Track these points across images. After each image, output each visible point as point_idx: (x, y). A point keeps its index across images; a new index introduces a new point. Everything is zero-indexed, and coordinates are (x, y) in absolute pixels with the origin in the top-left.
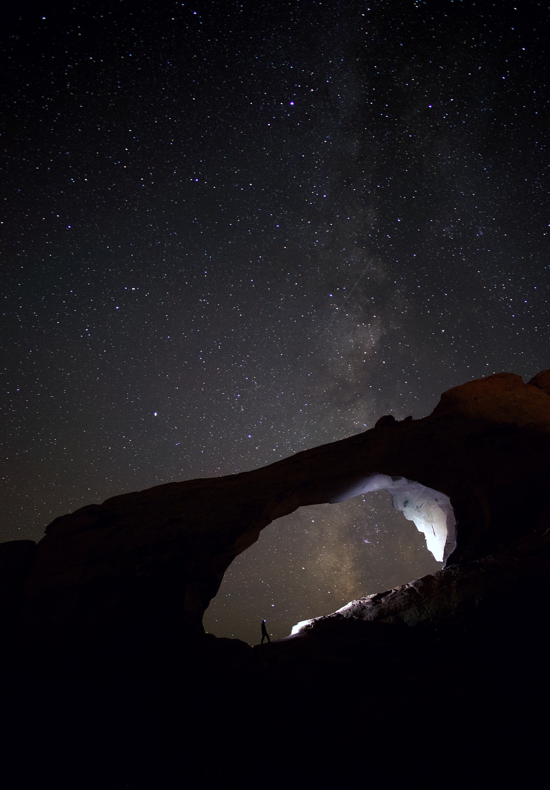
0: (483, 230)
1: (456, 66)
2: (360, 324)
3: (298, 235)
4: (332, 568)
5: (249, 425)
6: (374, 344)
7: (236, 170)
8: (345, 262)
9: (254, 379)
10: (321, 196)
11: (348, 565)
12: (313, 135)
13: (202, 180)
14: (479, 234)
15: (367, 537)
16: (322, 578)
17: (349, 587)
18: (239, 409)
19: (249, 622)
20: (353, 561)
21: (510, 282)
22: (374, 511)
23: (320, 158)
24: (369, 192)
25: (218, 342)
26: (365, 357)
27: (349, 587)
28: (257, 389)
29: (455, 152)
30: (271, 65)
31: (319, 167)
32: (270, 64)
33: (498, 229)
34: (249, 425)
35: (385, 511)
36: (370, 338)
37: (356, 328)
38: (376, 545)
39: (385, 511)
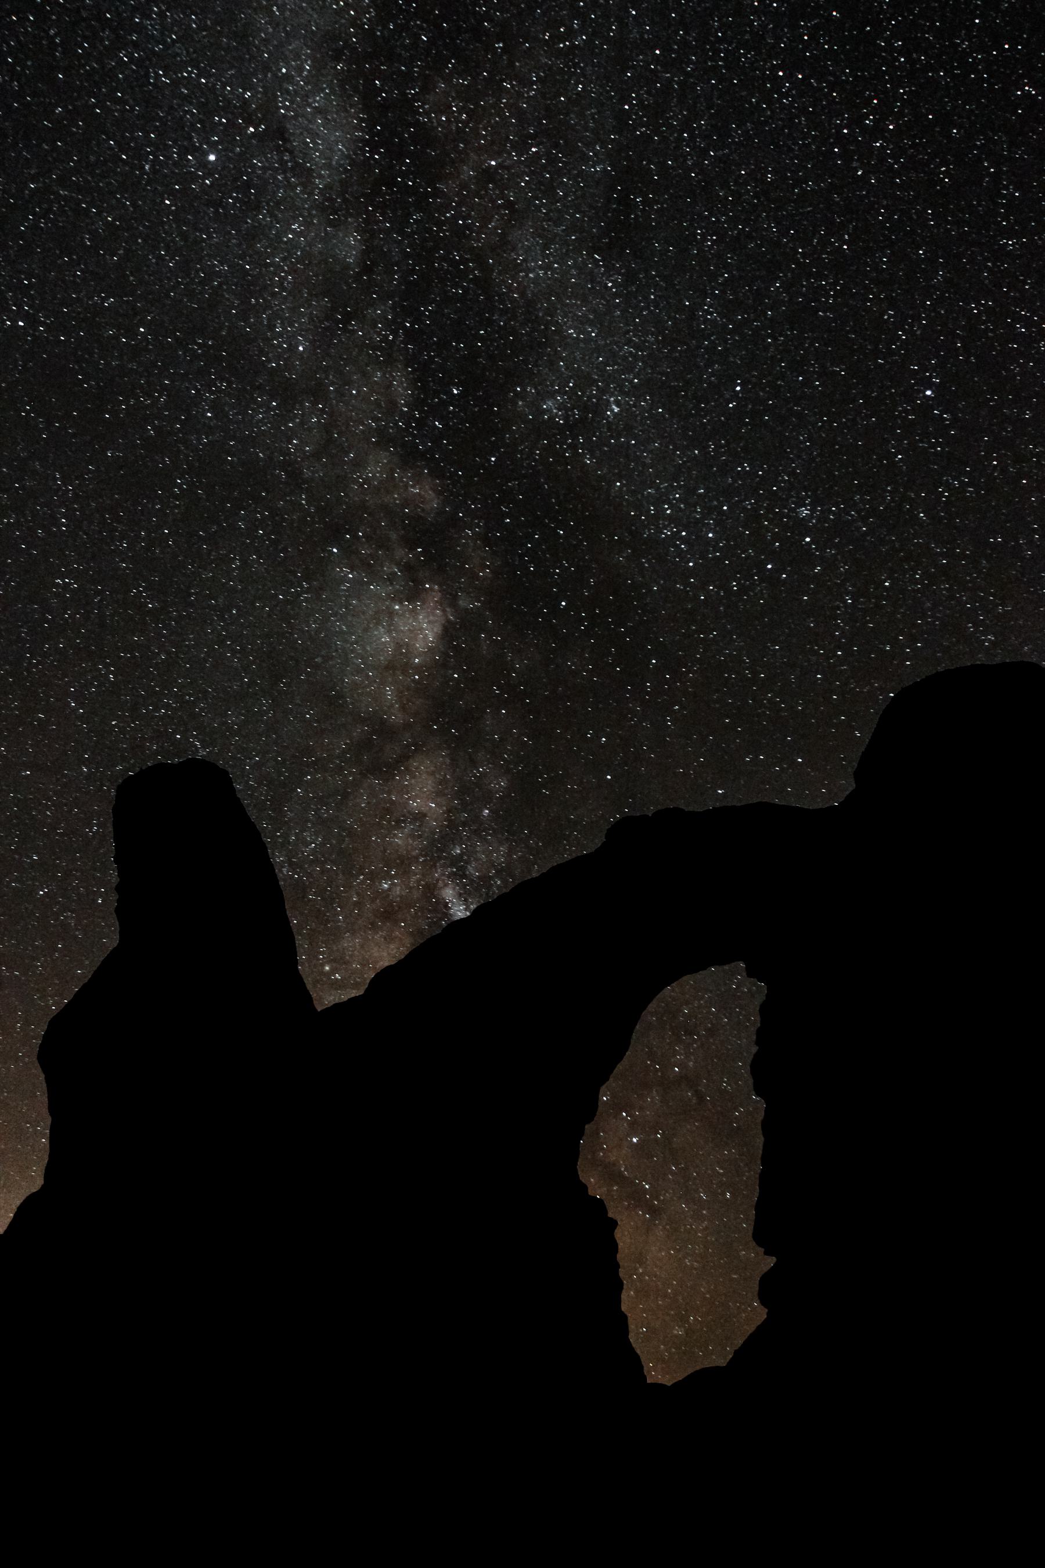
1: (534, 83)
2: (401, 603)
3: (253, 432)
6: (432, 642)
7: (104, 300)
8: (356, 481)
9: (195, 737)
10: (293, 348)
13: (32, 321)
14: (612, 411)
24: (391, 337)
25: (107, 666)
26: (418, 669)
30: (157, 76)
31: (283, 289)
32: (157, 74)
36: (421, 629)
37: (391, 613)
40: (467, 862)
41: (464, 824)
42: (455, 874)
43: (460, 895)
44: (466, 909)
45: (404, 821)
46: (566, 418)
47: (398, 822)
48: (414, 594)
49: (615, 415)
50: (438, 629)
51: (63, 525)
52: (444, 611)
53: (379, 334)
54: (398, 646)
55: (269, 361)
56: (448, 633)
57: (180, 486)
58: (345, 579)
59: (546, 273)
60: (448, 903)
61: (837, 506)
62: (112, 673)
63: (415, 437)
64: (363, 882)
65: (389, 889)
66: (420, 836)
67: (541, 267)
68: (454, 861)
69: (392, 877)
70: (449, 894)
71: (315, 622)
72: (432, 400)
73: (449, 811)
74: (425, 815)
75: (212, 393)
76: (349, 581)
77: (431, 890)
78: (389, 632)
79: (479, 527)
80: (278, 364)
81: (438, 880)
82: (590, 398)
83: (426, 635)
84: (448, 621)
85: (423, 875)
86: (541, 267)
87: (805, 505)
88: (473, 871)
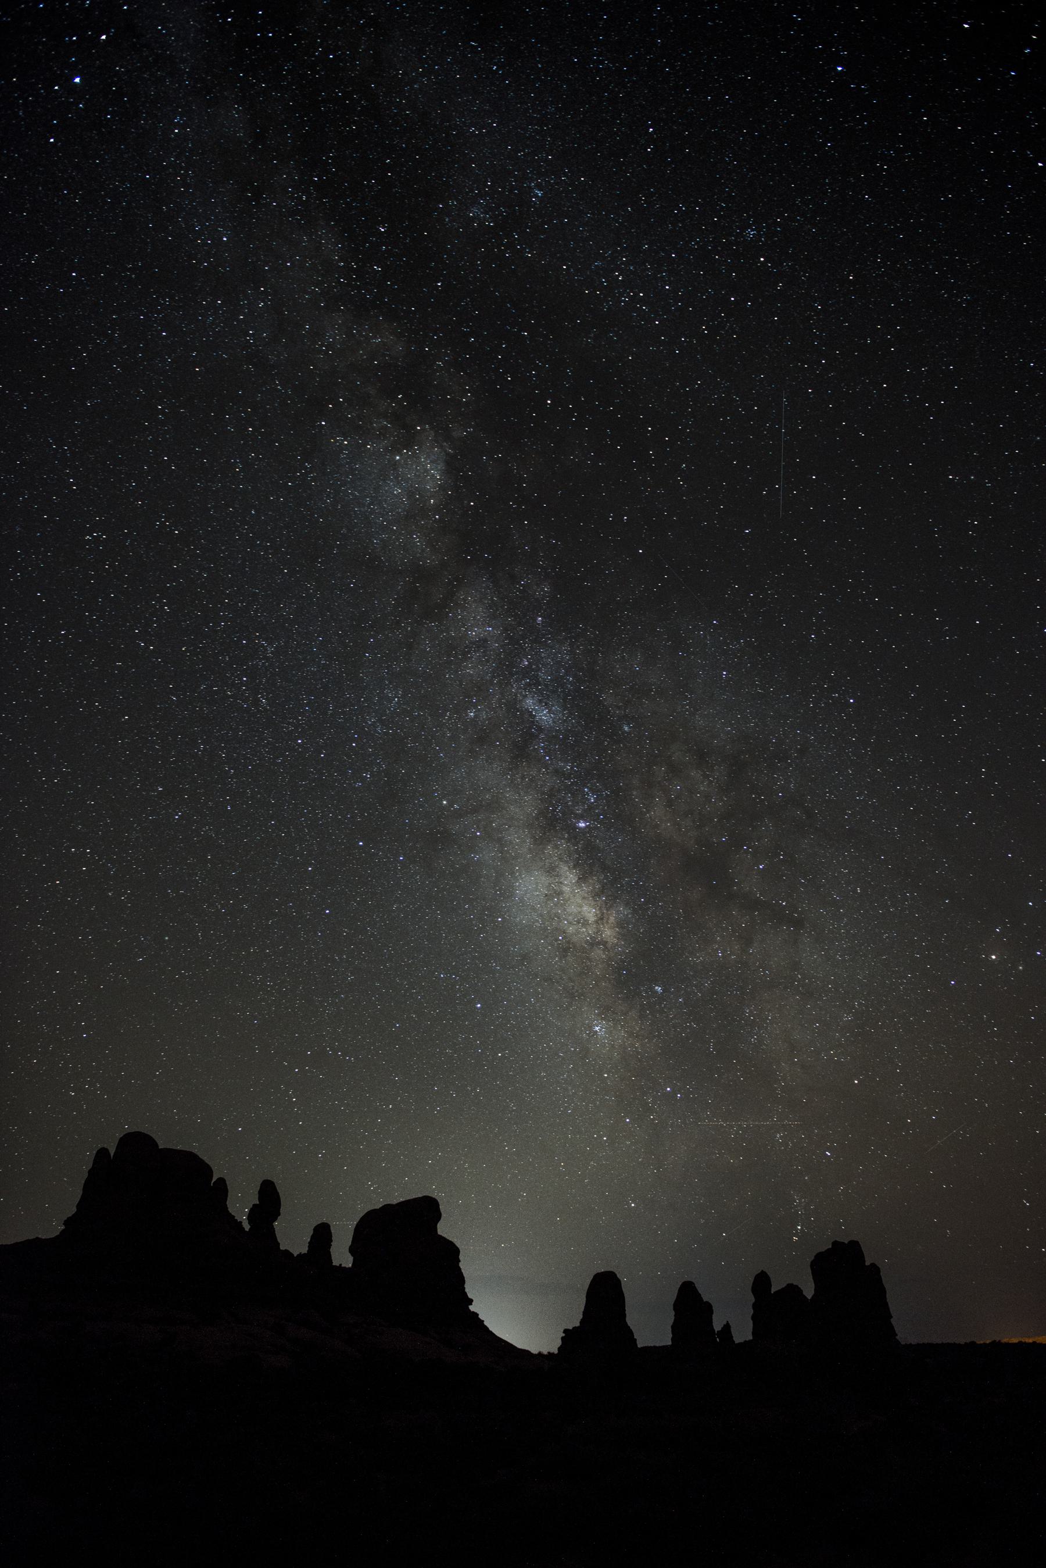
0: (539, 187)
4: (546, 895)
5: (289, 723)
6: (440, 479)
7: (30, 258)
8: (320, 351)
11: (569, 877)
12: (148, 127)
14: (536, 196)
15: (581, 817)
16: (538, 921)
17: (589, 912)
18: (256, 702)
19: (451, 1053)
20: (575, 867)
21: (625, 263)
22: (572, 768)
23: (182, 168)
26: (436, 509)
27: (589, 912)
28: (272, 653)
29: (428, 57)
31: (187, 186)
33: (565, 174)
34: (289, 723)
35: (588, 759)
36: (427, 471)
37: (395, 465)
38: (601, 822)
39: (588, 759)
40: (539, 670)
41: (523, 637)
42: (528, 685)
43: (540, 701)
44: (549, 712)
45: (469, 652)
46: (494, 218)
47: (464, 654)
48: (409, 440)
49: (541, 199)
50: (441, 466)
51: (73, 484)
52: (441, 447)
53: (292, 198)
54: (410, 495)
55: (201, 263)
56: (452, 467)
57: (162, 412)
58: (342, 447)
59: (429, 79)
60: (532, 712)
61: (781, 216)
62: (165, 604)
63: (359, 288)
64: (450, 718)
65: (476, 716)
66: (487, 661)
67: (422, 75)
68: (526, 672)
69: (475, 706)
70: (530, 703)
71: (328, 497)
72: (364, 247)
73: (506, 630)
74: (485, 640)
75: (159, 312)
76: (346, 447)
77: (513, 706)
78: (398, 484)
79: (448, 355)
80: (209, 262)
81: (516, 695)
82: (511, 191)
83: (433, 475)
84: (448, 454)
85: (502, 694)
86: (422, 75)
87: (750, 226)
88: (544, 676)
